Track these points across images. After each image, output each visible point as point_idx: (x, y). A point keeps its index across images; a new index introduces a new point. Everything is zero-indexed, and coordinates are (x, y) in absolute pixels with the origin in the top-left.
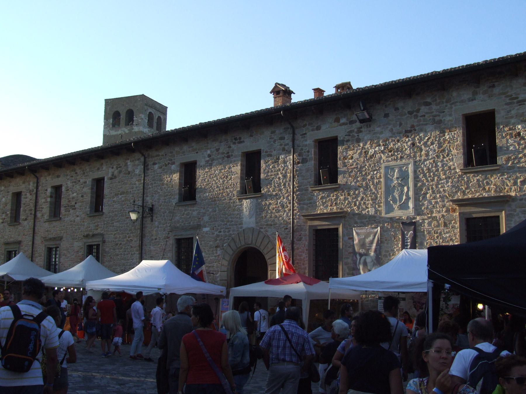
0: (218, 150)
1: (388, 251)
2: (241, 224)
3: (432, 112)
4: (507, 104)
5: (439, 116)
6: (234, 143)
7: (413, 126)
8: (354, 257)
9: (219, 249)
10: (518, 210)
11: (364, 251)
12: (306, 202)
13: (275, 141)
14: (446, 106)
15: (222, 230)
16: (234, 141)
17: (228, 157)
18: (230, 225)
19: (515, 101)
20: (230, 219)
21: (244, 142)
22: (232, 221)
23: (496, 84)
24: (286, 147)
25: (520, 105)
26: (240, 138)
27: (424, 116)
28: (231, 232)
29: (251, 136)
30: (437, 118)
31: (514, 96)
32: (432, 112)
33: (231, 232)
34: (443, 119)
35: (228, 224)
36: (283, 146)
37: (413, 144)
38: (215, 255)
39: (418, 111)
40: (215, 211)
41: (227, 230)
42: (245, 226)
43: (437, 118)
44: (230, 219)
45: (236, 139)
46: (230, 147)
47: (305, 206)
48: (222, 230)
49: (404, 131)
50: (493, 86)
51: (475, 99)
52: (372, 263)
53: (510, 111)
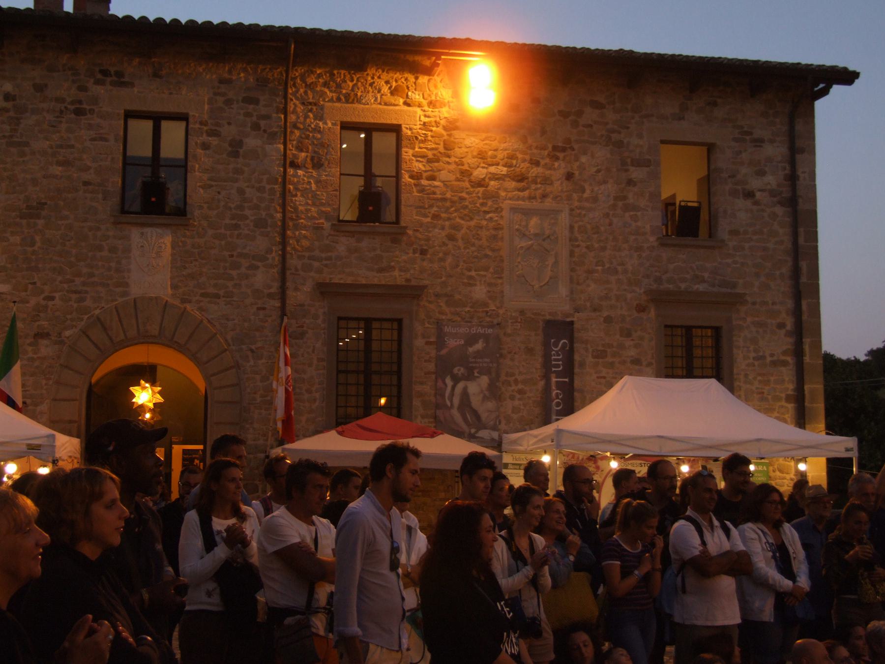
0: (40, 88)
1: (513, 375)
2: (127, 285)
3: (607, 124)
4: (736, 140)
5: (620, 133)
6: (98, 82)
7: (568, 141)
8: (440, 384)
9: (45, 342)
10: (749, 320)
11: (462, 370)
12: (317, 253)
13: (228, 102)
14: (633, 118)
15: (57, 295)
16: (99, 76)
17: (79, 112)
18: (84, 284)
19: (748, 138)
20: (85, 270)
21: (132, 85)
22: (91, 275)
23: (719, 101)
24: (263, 123)
25: (756, 146)
26: (120, 74)
27: (591, 126)
28: (88, 303)
29: (156, 75)
30: (615, 137)
31: (745, 129)
32: (607, 124)
33: (88, 303)
34: (625, 141)
35: (78, 281)
36: (254, 119)
37: (569, 176)
38: (30, 355)
39: (580, 113)
40: (33, 244)
41: (74, 296)
42: (136, 291)
43: (615, 137)
44: (85, 270)
45: (105, 73)
46: (83, 88)
47: (316, 264)
48: (57, 295)
49: (550, 146)
50: (715, 104)
51: (683, 118)
52: (482, 395)
53: (741, 152)
